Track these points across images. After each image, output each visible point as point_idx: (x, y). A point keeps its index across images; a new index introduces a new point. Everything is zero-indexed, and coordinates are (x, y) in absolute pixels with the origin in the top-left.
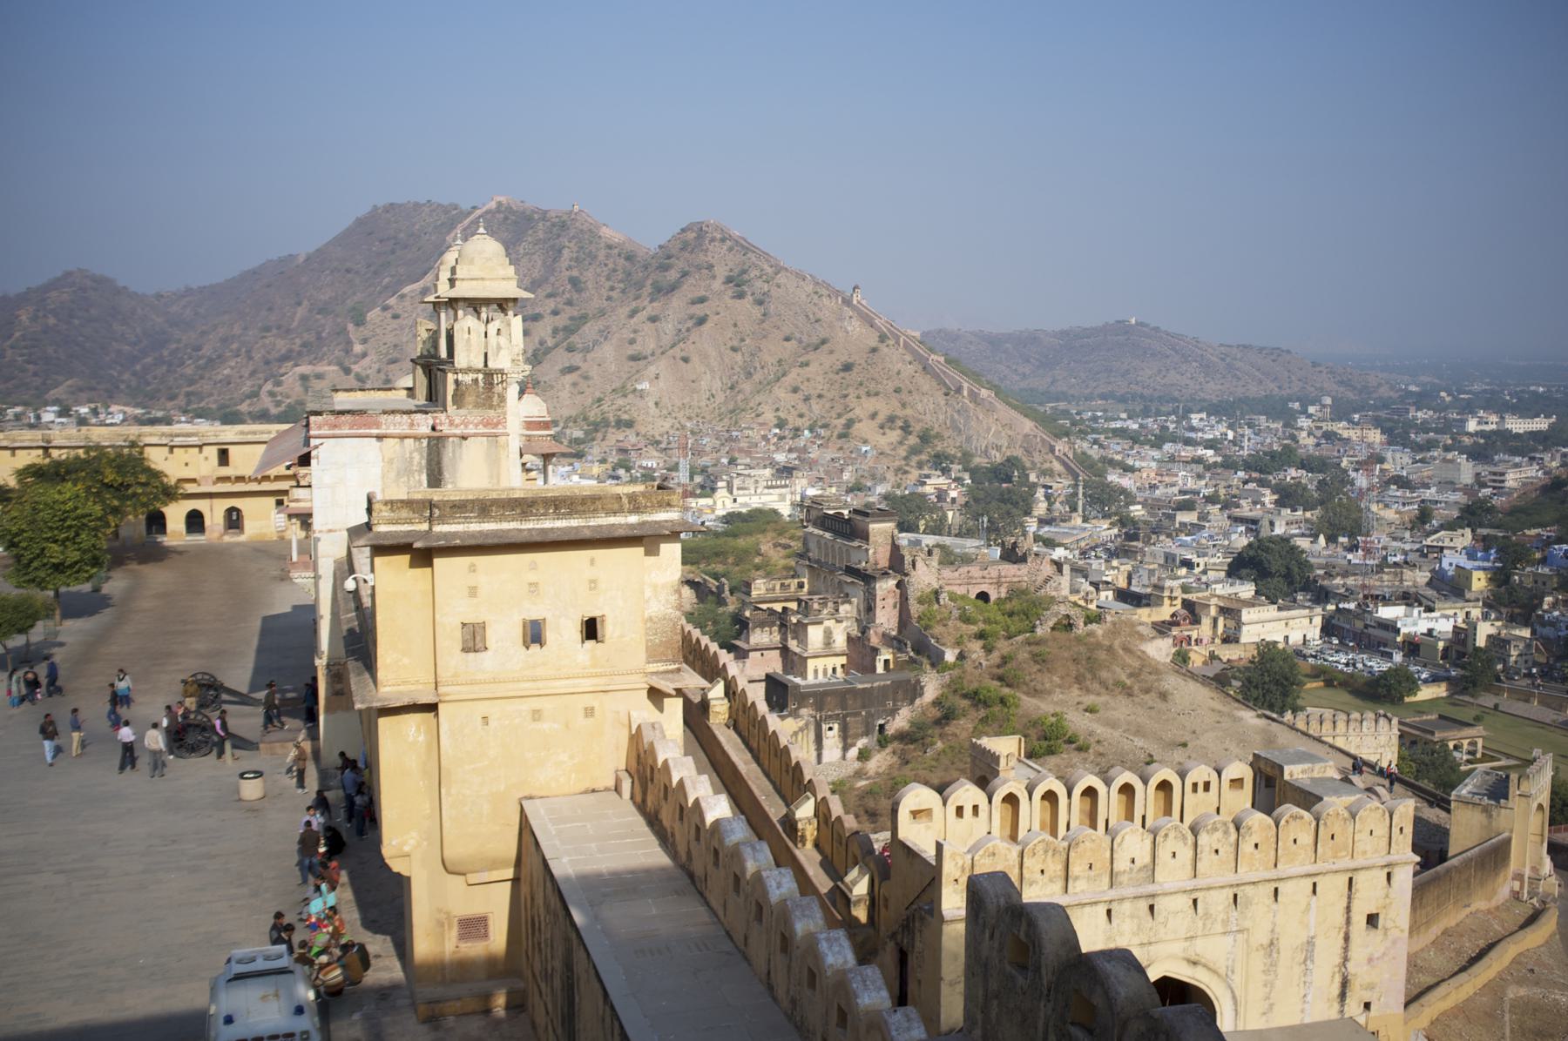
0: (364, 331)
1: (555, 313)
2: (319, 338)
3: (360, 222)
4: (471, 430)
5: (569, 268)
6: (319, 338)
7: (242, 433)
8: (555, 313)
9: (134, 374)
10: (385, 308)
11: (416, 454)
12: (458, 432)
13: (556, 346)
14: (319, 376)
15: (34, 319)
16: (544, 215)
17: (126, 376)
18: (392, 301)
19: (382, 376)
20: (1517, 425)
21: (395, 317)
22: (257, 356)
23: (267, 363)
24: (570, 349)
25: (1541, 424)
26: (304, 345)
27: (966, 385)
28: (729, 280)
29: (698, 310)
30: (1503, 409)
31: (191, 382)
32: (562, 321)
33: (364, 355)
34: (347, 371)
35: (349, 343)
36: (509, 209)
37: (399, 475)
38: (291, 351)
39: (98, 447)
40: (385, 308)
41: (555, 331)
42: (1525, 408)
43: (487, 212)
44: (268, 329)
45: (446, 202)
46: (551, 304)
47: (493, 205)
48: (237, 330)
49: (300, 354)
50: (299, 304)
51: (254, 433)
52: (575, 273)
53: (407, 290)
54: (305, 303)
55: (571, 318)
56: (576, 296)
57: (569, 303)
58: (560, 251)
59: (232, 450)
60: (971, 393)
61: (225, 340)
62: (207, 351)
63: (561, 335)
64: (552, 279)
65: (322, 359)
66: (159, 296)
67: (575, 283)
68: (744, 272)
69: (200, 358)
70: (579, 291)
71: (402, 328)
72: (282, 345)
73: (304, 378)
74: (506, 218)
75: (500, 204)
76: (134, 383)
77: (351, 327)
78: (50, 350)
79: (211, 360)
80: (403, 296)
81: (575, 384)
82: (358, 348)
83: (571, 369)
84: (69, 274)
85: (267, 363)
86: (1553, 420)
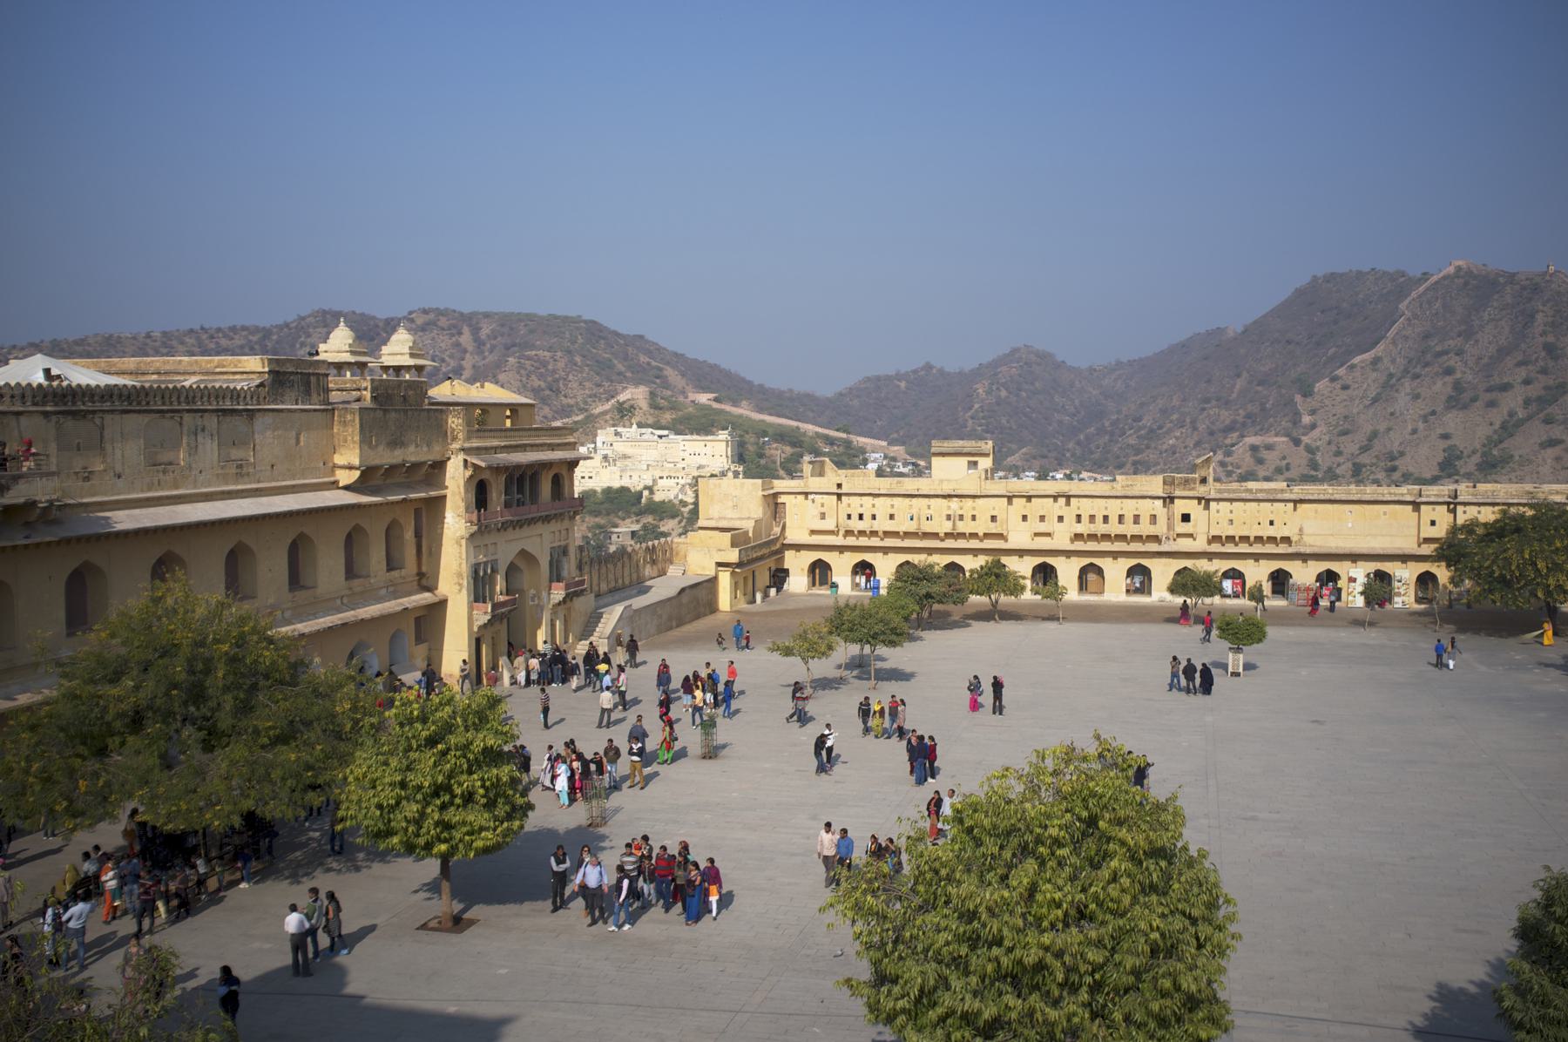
0: (1312, 402)
1: (1527, 382)
2: (1263, 409)
3: (1299, 293)
5: (1544, 334)
6: (1263, 409)
8: (1527, 382)
9: (1079, 443)
10: (1333, 379)
13: (1529, 418)
14: (1269, 447)
15: (988, 393)
16: (1512, 278)
17: (1071, 445)
18: (1341, 372)
19: (1334, 448)
21: (1345, 388)
22: (1202, 427)
23: (1212, 434)
24: (1548, 421)
26: (1248, 416)
31: (1138, 452)
32: (1534, 391)
33: (1313, 426)
34: (1297, 442)
35: (1297, 414)
36: (1469, 273)
38: (1234, 422)
39: (1550, 506)
40: (1333, 379)
41: (1527, 402)
43: (1444, 278)
44: (1207, 401)
45: (1391, 269)
46: (1523, 373)
47: (1451, 270)
48: (1176, 402)
49: (1244, 425)
50: (1238, 376)
52: (1550, 339)
53: (1357, 360)
54: (1245, 374)
55: (1546, 388)
56: (1551, 364)
57: (1544, 371)
58: (1532, 316)
61: (1164, 411)
62: (1147, 421)
63: (1533, 407)
64: (1523, 346)
65: (1268, 430)
66: (1092, 370)
67: (1550, 349)
69: (1140, 429)
70: (1556, 358)
71: (1352, 399)
72: (1226, 416)
73: (1254, 448)
74: (1466, 284)
75: (1459, 269)
76: (1078, 452)
77: (1298, 398)
78: (1004, 421)
79: (1151, 431)
80: (1352, 367)
81: (1558, 459)
82: (1306, 419)
83: (1552, 443)
84: (1015, 351)
85: (1212, 434)
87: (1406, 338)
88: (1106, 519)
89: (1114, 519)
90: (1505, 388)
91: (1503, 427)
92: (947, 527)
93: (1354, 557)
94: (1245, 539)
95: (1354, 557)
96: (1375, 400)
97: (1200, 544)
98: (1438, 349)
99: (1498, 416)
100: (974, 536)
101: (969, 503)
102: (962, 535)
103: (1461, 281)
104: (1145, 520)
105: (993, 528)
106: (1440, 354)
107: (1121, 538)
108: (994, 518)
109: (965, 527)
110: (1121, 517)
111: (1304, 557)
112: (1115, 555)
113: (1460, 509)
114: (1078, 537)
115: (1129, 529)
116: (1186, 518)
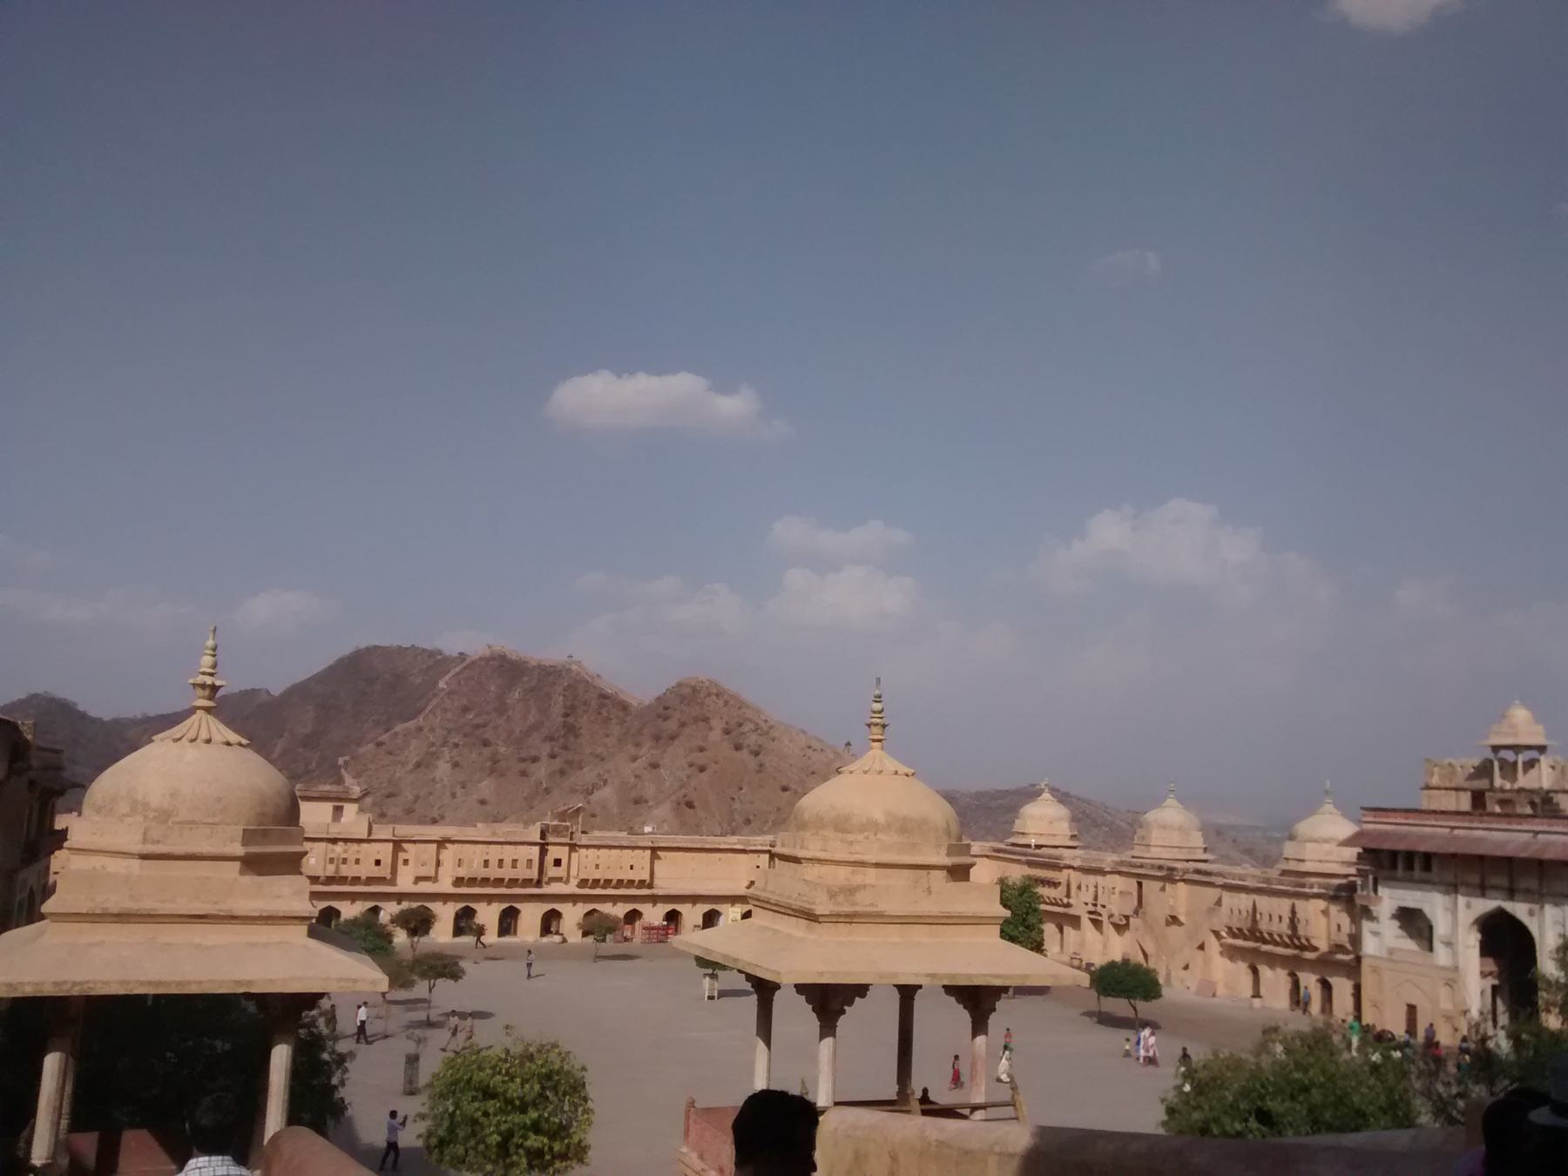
18: (384, 737)
21: (390, 753)
53: (399, 728)
80: (396, 734)
87: (445, 710)
88: (486, 863)
89: (494, 863)
92: (331, 870)
93: (694, 899)
94: (608, 883)
95: (694, 899)
96: (418, 765)
97: (571, 888)
98: (479, 721)
100: (356, 880)
101: (355, 847)
102: (343, 880)
104: (522, 864)
105: (377, 872)
106: (478, 726)
107: (499, 882)
108: (378, 863)
109: (346, 871)
110: (501, 861)
111: (654, 899)
112: (490, 899)
114: (459, 881)
115: (507, 873)
116: (558, 863)
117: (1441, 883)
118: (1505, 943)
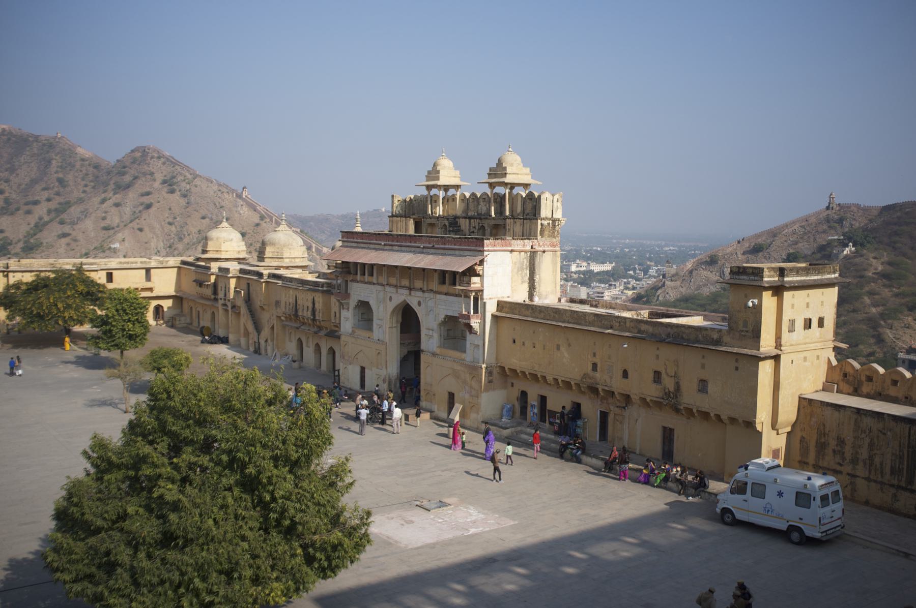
1: (49, 200)
4: (546, 249)
5: (57, 172)
7: (120, 263)
8: (49, 200)
11: (524, 259)
12: (541, 249)
13: (51, 221)
16: (37, 138)
20: (596, 268)
24: (62, 223)
25: (607, 267)
27: (314, 245)
28: (164, 182)
29: (146, 200)
30: (588, 259)
32: (53, 205)
36: (10, 133)
37: (518, 271)
39: (64, 272)
41: (49, 212)
42: (601, 258)
46: (46, 194)
51: (128, 263)
52: (61, 175)
55: (60, 204)
56: (62, 190)
57: (58, 194)
59: (115, 272)
60: (317, 249)
63: (53, 215)
64: (45, 179)
67: (61, 181)
68: (174, 177)
70: (64, 187)
74: (9, 139)
81: (68, 244)
83: (65, 235)
86: (614, 265)
90: (36, 203)
91: (36, 226)
99: (32, 220)
103: (6, 137)
113: (11, 275)
117: (378, 284)
118: (408, 320)
